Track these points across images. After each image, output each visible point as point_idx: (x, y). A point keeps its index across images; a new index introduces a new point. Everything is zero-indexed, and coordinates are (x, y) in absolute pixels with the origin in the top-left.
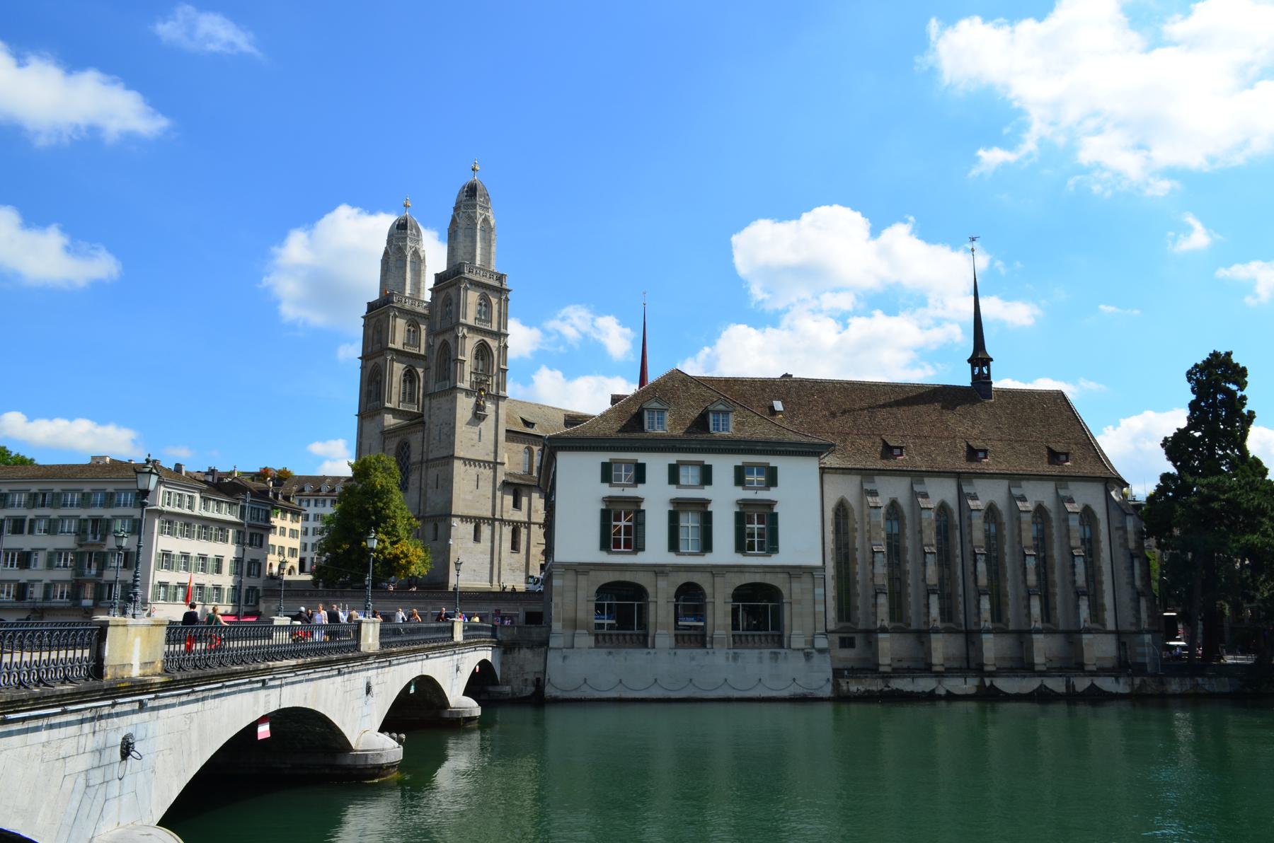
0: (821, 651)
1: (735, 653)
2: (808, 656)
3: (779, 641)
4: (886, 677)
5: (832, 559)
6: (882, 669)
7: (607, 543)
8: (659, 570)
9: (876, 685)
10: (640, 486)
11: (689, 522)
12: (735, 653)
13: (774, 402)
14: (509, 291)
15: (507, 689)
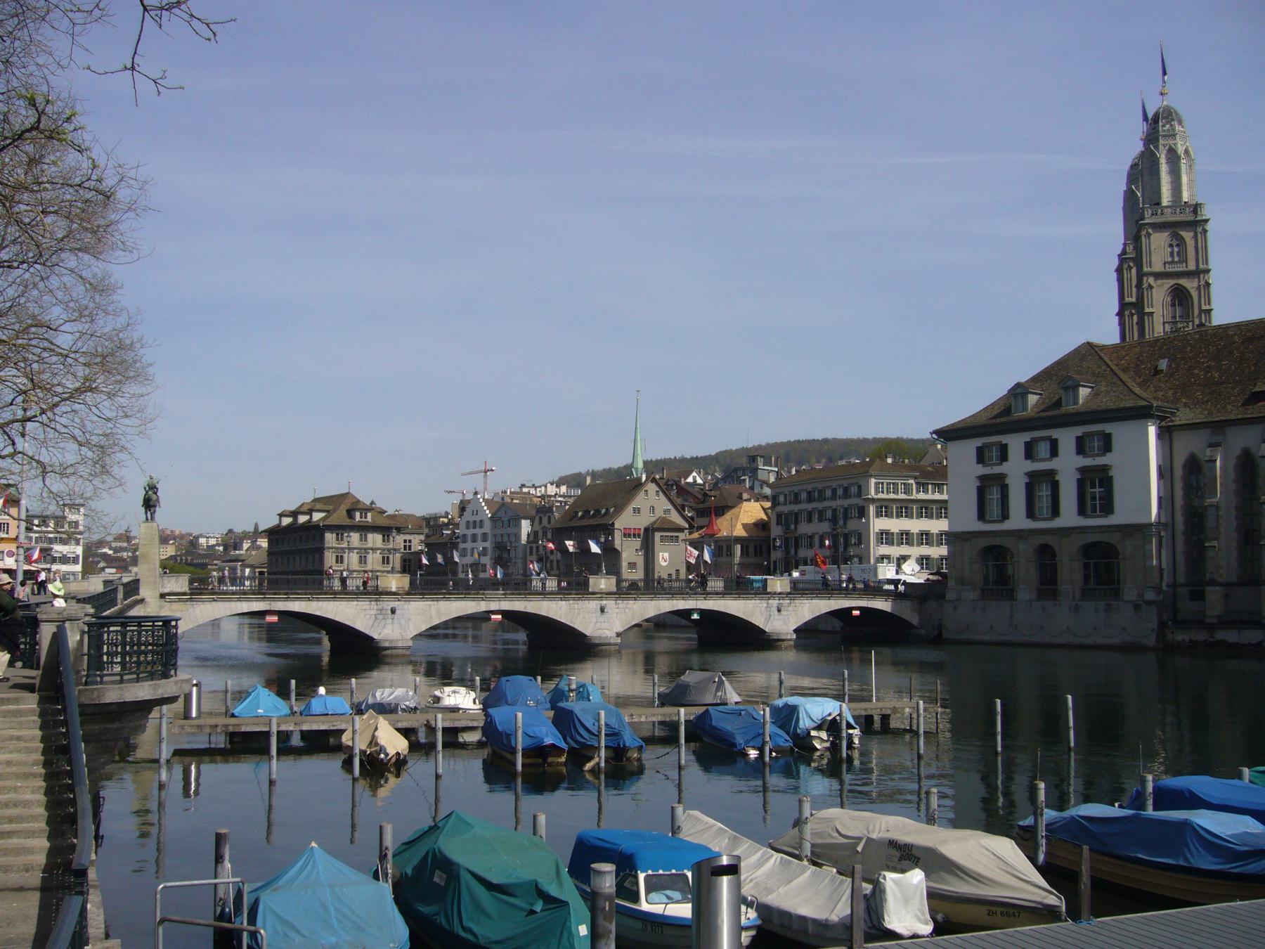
0: (1149, 603)
1: (1076, 605)
2: (1137, 608)
3: (1116, 593)
4: (1211, 628)
5: (1182, 515)
6: (1208, 621)
7: (981, 516)
8: (1020, 534)
9: (1200, 636)
10: (1055, 459)
11: (1044, 492)
12: (1076, 605)
13: (1167, 360)
14: (1207, 221)
15: (923, 632)
